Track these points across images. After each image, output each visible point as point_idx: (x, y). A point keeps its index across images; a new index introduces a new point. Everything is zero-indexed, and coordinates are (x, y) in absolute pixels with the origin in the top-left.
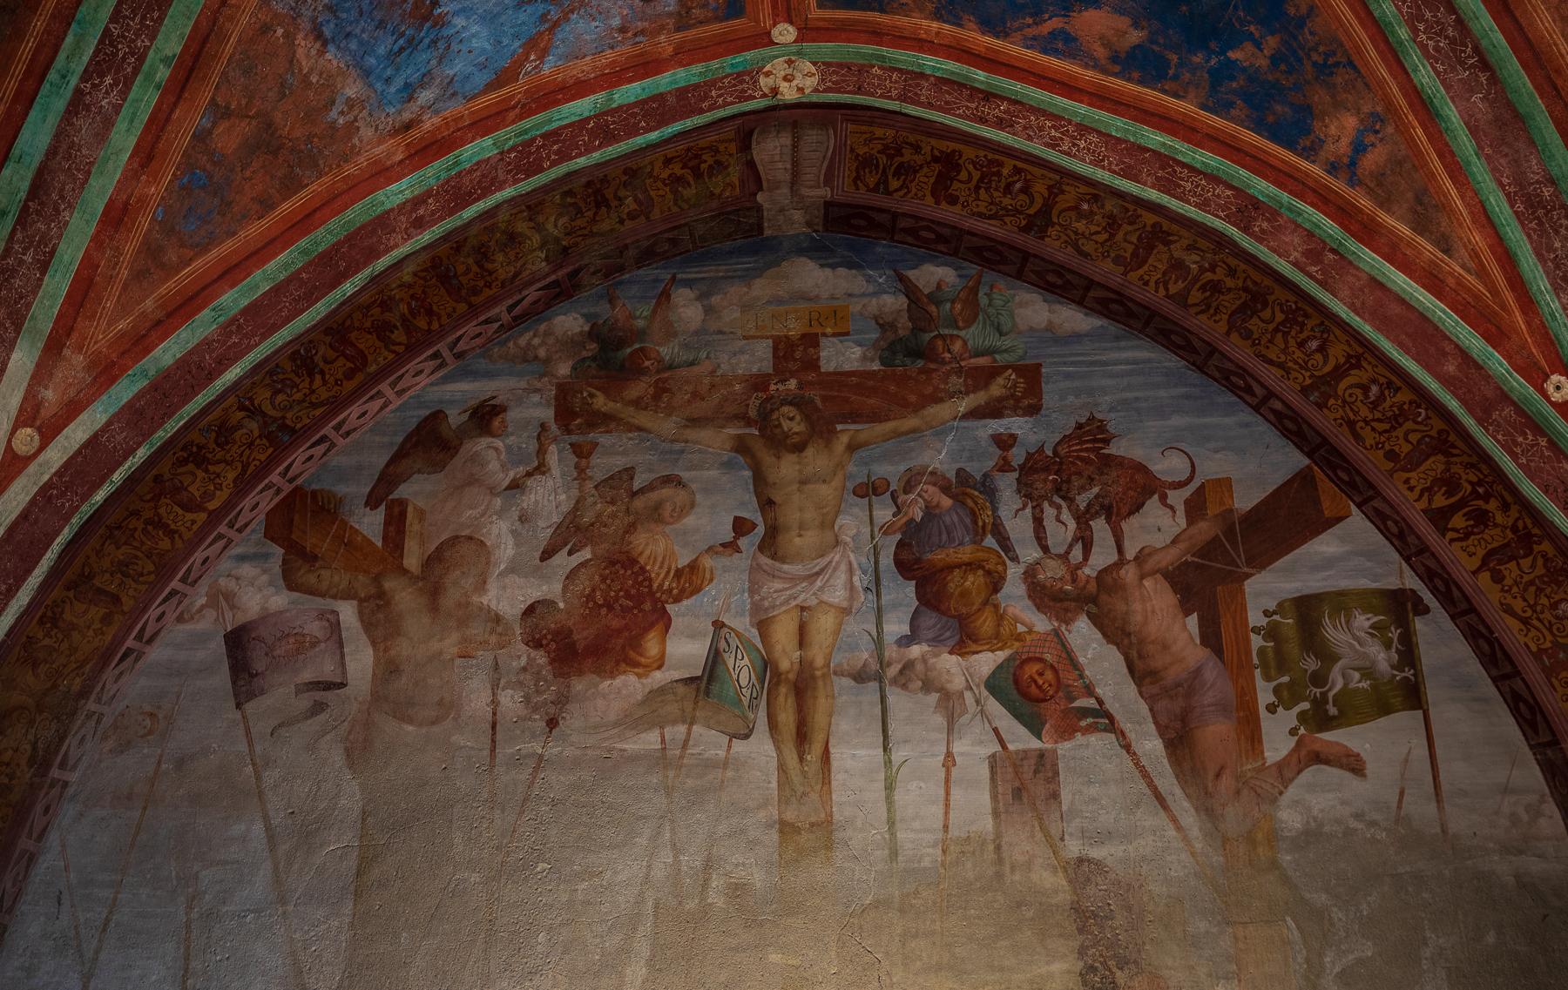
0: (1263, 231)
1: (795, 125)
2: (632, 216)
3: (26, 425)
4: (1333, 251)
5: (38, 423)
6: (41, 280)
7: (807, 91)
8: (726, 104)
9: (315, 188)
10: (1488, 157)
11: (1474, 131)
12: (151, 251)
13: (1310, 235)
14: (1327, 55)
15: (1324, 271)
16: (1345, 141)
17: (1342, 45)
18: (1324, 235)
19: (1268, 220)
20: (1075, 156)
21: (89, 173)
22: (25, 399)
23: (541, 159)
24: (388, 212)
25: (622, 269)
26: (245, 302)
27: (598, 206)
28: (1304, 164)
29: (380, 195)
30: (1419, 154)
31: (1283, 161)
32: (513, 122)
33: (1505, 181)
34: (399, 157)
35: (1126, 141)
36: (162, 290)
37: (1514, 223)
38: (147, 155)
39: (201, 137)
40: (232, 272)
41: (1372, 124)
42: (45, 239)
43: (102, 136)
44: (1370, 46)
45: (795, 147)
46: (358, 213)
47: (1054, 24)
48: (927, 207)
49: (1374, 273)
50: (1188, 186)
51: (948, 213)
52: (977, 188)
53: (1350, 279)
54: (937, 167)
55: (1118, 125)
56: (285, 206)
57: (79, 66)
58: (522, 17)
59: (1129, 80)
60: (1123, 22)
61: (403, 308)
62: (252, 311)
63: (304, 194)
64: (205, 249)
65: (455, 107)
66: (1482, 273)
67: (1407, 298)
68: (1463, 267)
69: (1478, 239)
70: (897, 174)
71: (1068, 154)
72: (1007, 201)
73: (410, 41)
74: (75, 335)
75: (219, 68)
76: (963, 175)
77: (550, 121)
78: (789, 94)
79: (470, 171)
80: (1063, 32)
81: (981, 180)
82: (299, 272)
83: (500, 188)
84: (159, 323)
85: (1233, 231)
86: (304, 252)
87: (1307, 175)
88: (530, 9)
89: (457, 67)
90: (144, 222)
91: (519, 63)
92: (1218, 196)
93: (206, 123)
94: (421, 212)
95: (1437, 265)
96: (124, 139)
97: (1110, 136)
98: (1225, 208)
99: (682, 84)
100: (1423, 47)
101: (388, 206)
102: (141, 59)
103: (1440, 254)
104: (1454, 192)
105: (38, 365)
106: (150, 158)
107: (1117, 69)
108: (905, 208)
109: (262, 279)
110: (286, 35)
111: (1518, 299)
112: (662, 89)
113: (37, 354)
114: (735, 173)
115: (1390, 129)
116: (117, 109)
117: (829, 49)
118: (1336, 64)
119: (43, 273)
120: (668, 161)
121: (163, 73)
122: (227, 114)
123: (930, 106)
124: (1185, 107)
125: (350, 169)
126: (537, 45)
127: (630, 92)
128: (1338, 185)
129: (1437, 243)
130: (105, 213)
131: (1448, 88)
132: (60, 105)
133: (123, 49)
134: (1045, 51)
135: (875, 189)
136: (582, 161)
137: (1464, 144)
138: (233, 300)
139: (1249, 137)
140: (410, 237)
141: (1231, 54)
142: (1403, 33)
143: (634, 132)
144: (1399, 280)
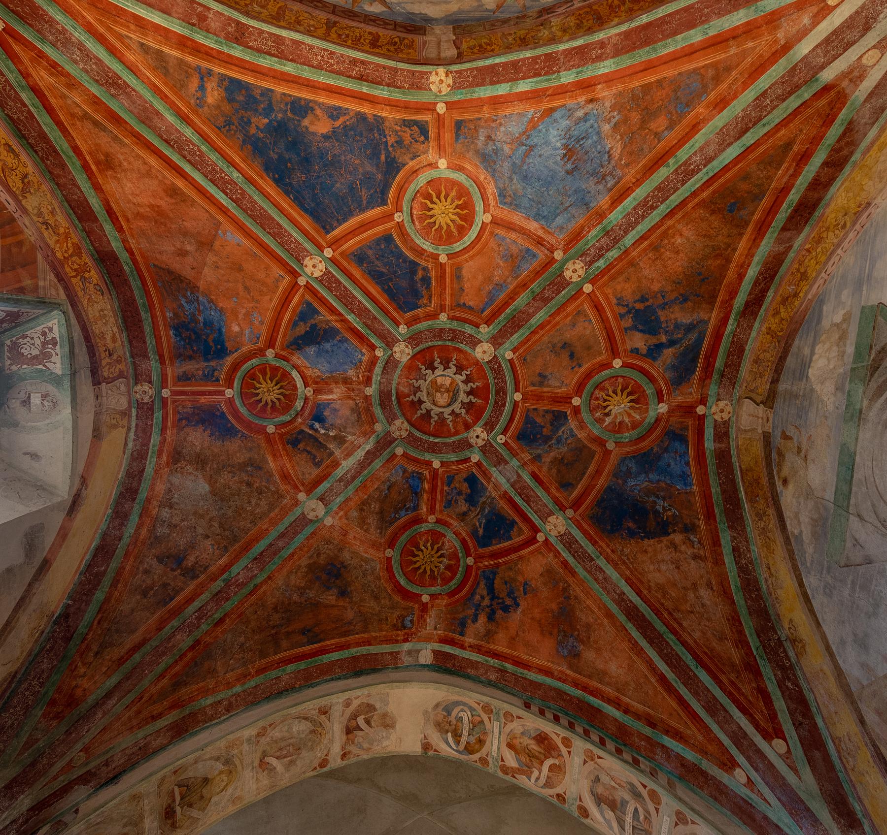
0: (230, 25)
1: (439, 59)
2: (511, 34)
3: (829, 6)
4: (194, 25)
5: (822, 5)
6: (769, 88)
7: (434, 73)
8: (466, 70)
9: (636, 83)
10: (146, 102)
11: (158, 113)
12: (717, 79)
13: (208, 31)
14: (229, 130)
15: (194, 9)
16: (209, 89)
17: (226, 136)
18: (201, 32)
19: (229, 33)
20: (322, 49)
21: (721, 130)
22: (818, 24)
23: (545, 62)
24: (613, 57)
25: (518, 18)
26: (692, 32)
27: (524, 39)
28: (223, 71)
29: (614, 68)
30: (176, 93)
31: (232, 70)
32: (551, 87)
33: (133, 93)
34: (599, 87)
35: (301, 64)
36: (723, 56)
37: (119, 73)
38: (695, 128)
39: (670, 127)
40: (690, 52)
41: (201, 102)
42: (756, 107)
43: (707, 144)
44: (214, 139)
45: (439, 53)
46: (626, 61)
47: (338, 123)
48: (381, 32)
49: (170, 19)
50: (269, 43)
51: (373, 29)
52: (361, 37)
53: (180, 11)
54: (379, 44)
55: (307, 73)
56: (653, 80)
57: (700, 175)
58: (535, 140)
59: (305, 99)
60: (312, 129)
61: (622, 8)
62: (691, 26)
63: (643, 82)
64: (695, 70)
65: (571, 103)
66: (120, 38)
67: (149, 9)
68: (130, 38)
69: (130, 57)
70: (396, 43)
71: (325, 50)
72: (347, 32)
73: (579, 141)
74: (774, 50)
75: (651, 155)
76: (367, 41)
77: (536, 82)
78: (441, 70)
79: (573, 66)
80: (334, 120)
81: (359, 40)
82: (661, 40)
83: (564, 50)
84: (734, 38)
85: (244, 20)
86: (655, 50)
87: (220, 66)
88: (532, 143)
89: (565, 123)
90: (712, 96)
91: (541, 118)
92: (255, 40)
93: (666, 133)
94: (599, 52)
95: (143, 34)
96: (699, 139)
97: (308, 66)
98: (251, 34)
99: (482, 88)
100: (194, 145)
101: (612, 60)
102: (676, 170)
103: (144, 42)
104: (153, 79)
105: (800, 41)
106: (694, 126)
107: (311, 105)
108: (391, 32)
109: (679, 42)
110: (621, 160)
111: (96, 29)
112: (490, 87)
113: (796, 48)
114: (465, 46)
115: (192, 101)
116: (695, 154)
117: (423, 97)
118: (226, 126)
119: (767, 90)
120: (493, 50)
121: (671, 161)
122: (656, 134)
123: (384, 67)
124: (280, 89)
125: (620, 87)
126: (533, 125)
127: (502, 89)
128: (205, 65)
129: (149, 48)
130: (725, 108)
131: (177, 130)
132: (715, 163)
133: (680, 177)
134: (340, 108)
135: (404, 39)
136: (528, 54)
137: (159, 105)
138: (696, 36)
139: (249, 79)
140: (609, 38)
141: (266, 121)
142: (204, 148)
143: (505, 65)
144: (156, 18)
